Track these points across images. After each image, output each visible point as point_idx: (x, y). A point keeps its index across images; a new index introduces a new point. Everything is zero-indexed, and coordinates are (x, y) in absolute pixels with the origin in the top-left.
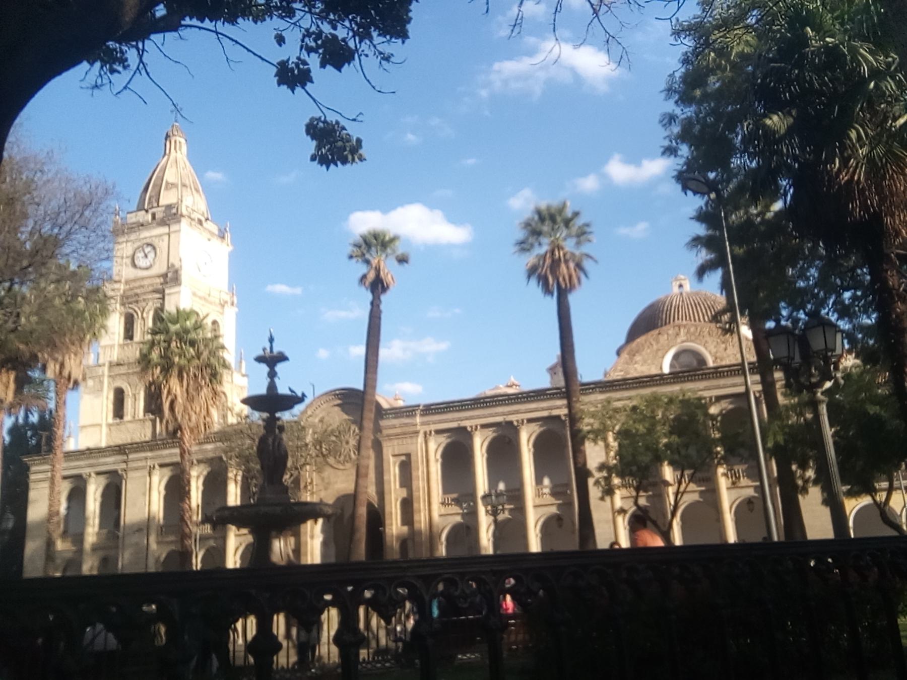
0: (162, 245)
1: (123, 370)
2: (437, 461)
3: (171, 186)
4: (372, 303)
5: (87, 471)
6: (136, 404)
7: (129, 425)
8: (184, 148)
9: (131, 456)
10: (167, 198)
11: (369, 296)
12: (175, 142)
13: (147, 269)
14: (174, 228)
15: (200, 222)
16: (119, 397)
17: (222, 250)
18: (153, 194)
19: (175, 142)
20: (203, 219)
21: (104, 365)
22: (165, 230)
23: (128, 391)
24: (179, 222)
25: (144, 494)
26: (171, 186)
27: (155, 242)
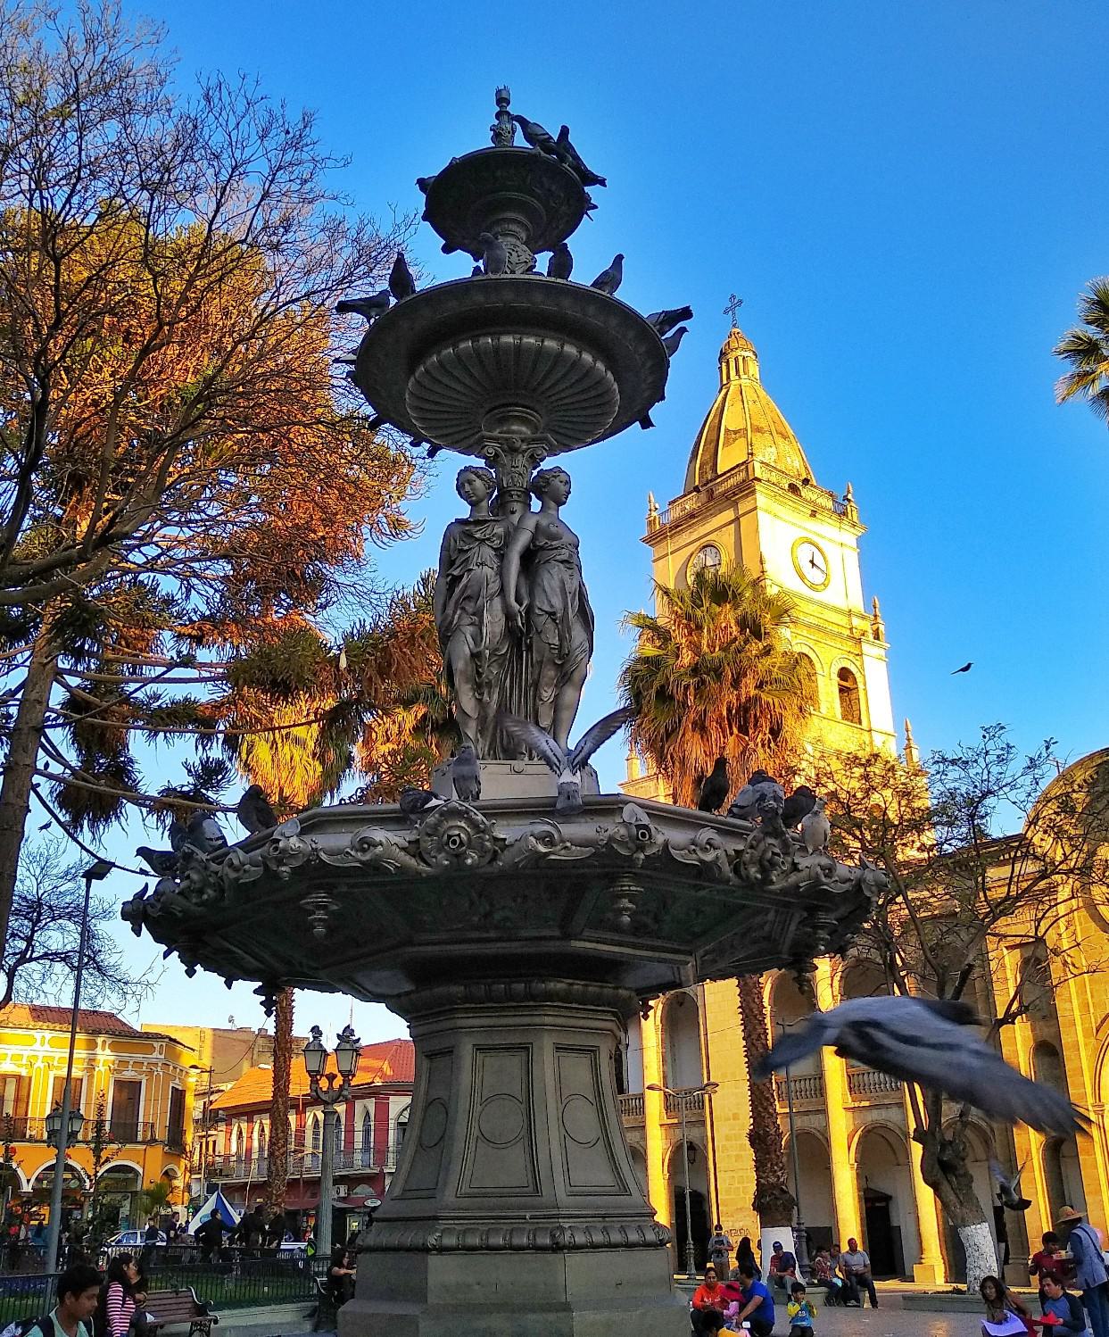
0: (726, 539)
8: (754, 369)
12: (736, 359)
14: (743, 506)
17: (840, 543)
19: (736, 359)
20: (799, 483)
22: (729, 515)
24: (753, 492)
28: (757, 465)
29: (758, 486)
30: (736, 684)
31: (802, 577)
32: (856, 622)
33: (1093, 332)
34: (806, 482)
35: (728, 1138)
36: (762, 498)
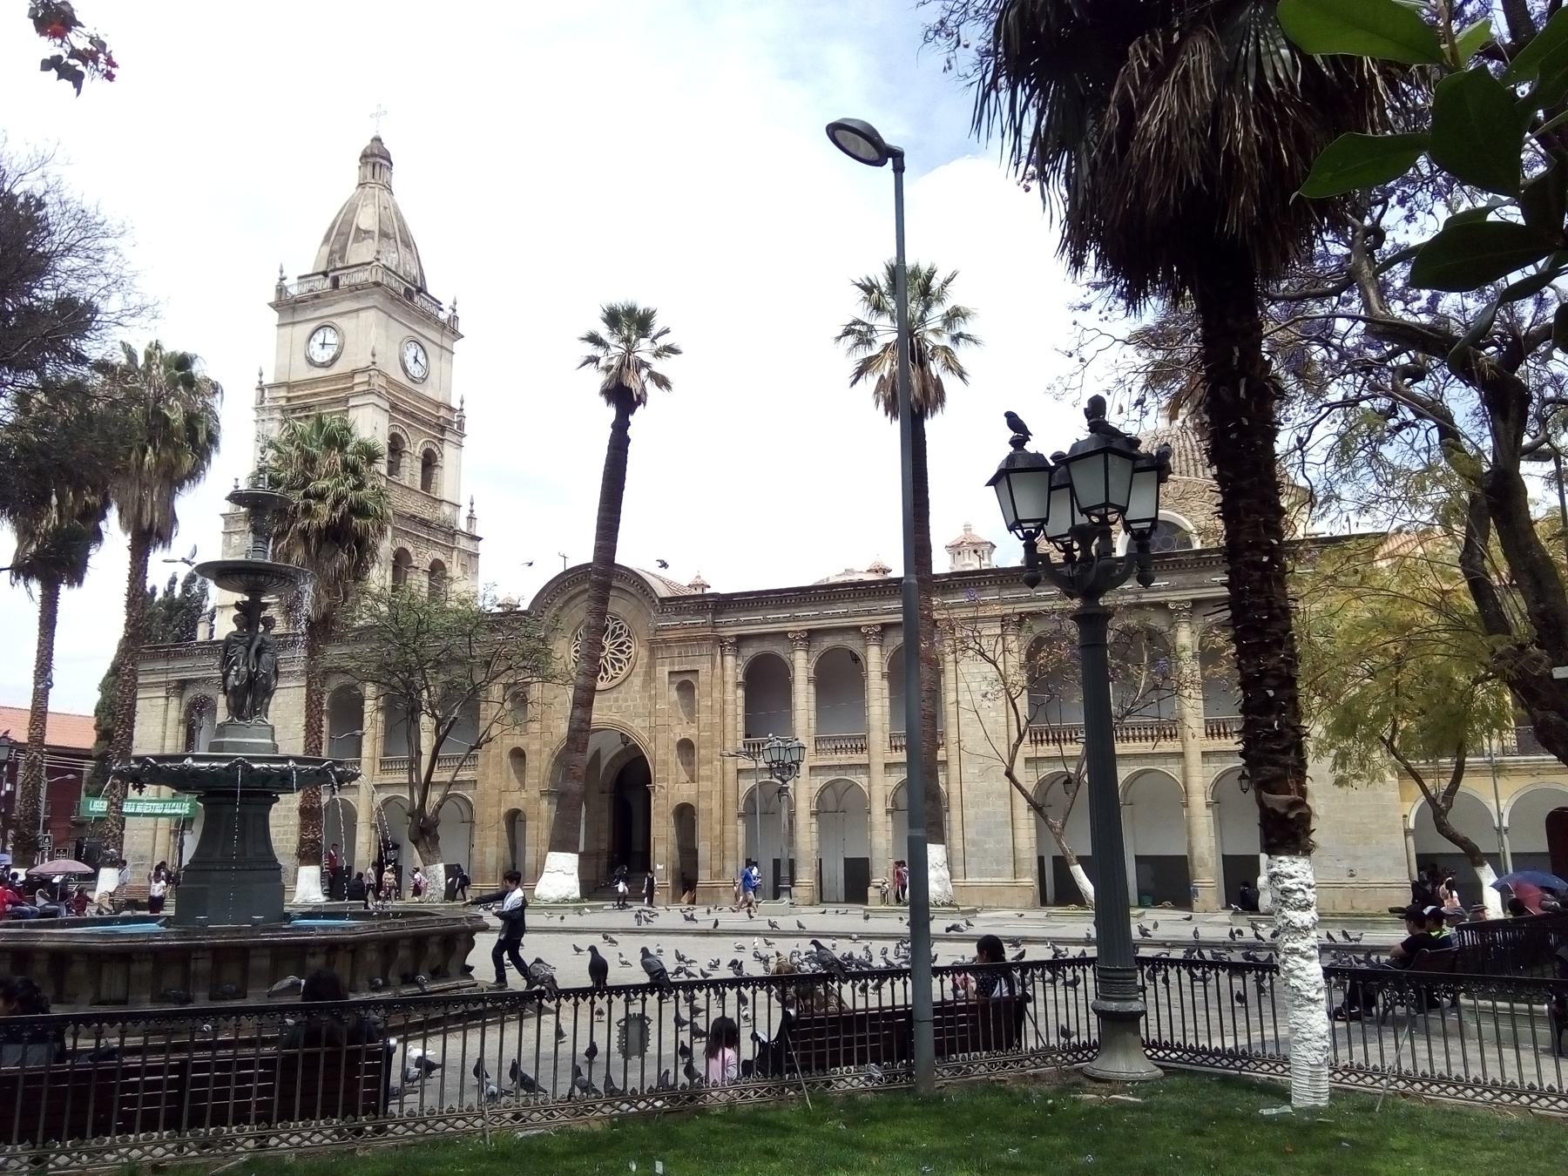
2: (738, 685)
4: (614, 426)
11: (610, 413)
13: (323, 365)
18: (337, 247)
26: (362, 234)
31: (405, 370)
32: (443, 412)
33: (603, 331)
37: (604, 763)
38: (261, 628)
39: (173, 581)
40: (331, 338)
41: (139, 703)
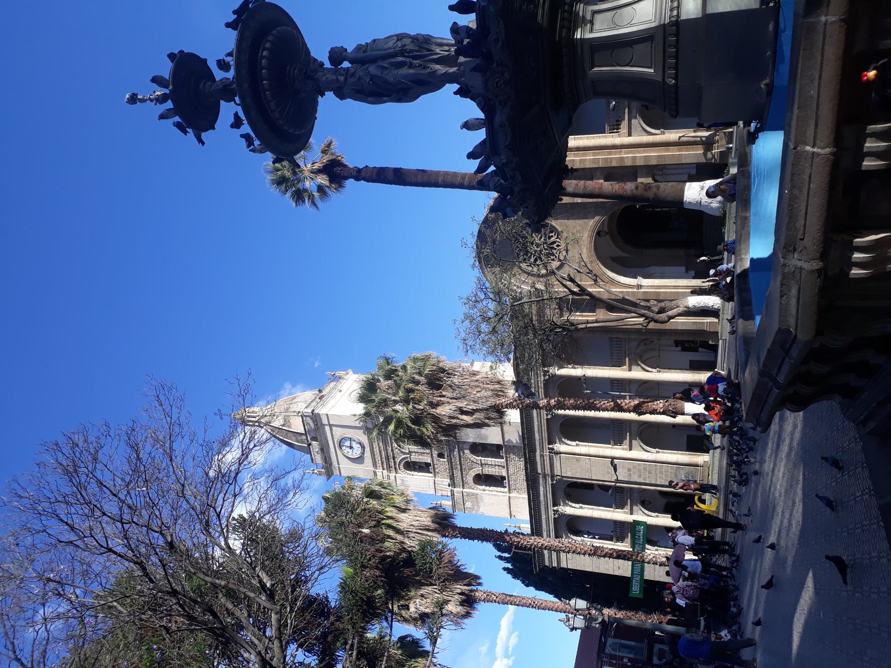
0: (338, 433)
1: (457, 474)
3: (286, 422)
5: (552, 516)
6: (493, 466)
7: (511, 471)
9: (539, 471)
10: (297, 426)
11: (350, 183)
13: (363, 447)
14: (325, 421)
15: (321, 398)
16: (484, 480)
21: (452, 491)
22: (327, 428)
23: (477, 470)
24: (319, 414)
25: (578, 460)
27: (337, 438)
28: (306, 410)
29: (316, 411)
30: (417, 383)
34: (320, 391)
35: (640, 476)
36: (322, 411)
37: (619, 253)
38: (346, 64)
39: (500, 558)
40: (348, 443)
41: (570, 567)
